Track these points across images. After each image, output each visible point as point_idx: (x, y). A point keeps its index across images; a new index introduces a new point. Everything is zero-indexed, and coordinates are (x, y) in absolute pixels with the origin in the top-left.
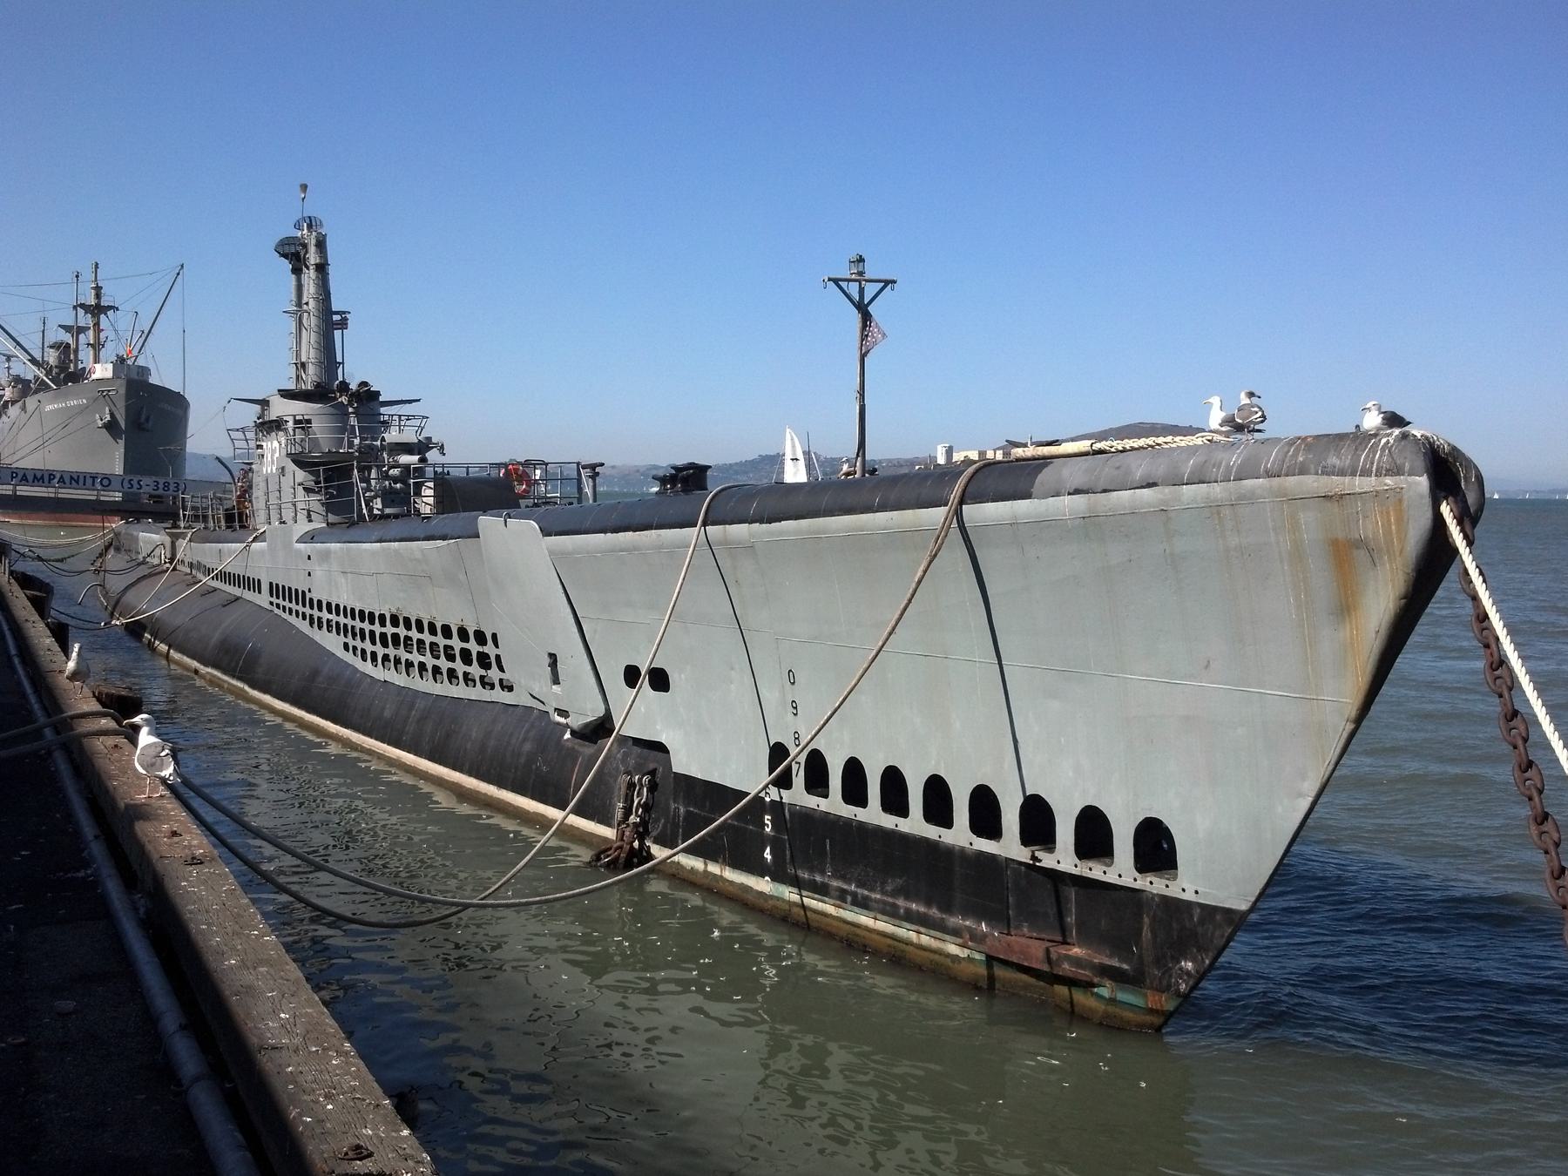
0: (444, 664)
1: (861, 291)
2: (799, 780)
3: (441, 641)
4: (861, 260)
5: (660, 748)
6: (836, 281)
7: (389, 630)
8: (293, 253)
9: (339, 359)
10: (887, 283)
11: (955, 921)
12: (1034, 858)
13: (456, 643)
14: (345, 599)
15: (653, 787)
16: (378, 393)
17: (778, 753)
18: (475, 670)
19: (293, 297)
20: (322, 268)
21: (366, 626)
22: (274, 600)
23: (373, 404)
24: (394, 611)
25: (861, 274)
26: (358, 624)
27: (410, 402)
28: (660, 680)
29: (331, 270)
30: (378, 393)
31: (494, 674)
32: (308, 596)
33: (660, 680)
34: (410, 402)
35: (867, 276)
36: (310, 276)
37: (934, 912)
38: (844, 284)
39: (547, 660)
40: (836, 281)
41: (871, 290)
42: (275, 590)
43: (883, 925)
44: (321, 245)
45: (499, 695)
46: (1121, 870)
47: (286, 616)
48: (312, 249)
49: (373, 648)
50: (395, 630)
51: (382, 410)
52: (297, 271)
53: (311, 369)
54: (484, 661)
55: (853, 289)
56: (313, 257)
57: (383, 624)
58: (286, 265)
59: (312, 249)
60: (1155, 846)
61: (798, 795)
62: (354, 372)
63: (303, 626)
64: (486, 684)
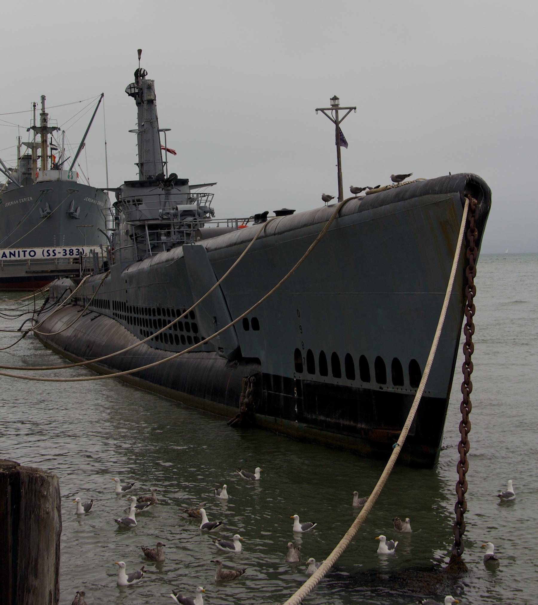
1: (337, 112)
2: (305, 367)
7: (157, 317)
9: (164, 160)
10: (351, 109)
12: (381, 388)
14: (141, 304)
17: (297, 353)
18: (192, 334)
22: (115, 311)
24: (158, 306)
27: (212, 184)
32: (127, 305)
33: (256, 325)
34: (212, 184)
40: (322, 110)
41: (342, 113)
44: (150, 87)
50: (159, 317)
51: (192, 191)
52: (138, 104)
57: (154, 315)
58: (132, 100)
61: (305, 376)
62: (174, 166)
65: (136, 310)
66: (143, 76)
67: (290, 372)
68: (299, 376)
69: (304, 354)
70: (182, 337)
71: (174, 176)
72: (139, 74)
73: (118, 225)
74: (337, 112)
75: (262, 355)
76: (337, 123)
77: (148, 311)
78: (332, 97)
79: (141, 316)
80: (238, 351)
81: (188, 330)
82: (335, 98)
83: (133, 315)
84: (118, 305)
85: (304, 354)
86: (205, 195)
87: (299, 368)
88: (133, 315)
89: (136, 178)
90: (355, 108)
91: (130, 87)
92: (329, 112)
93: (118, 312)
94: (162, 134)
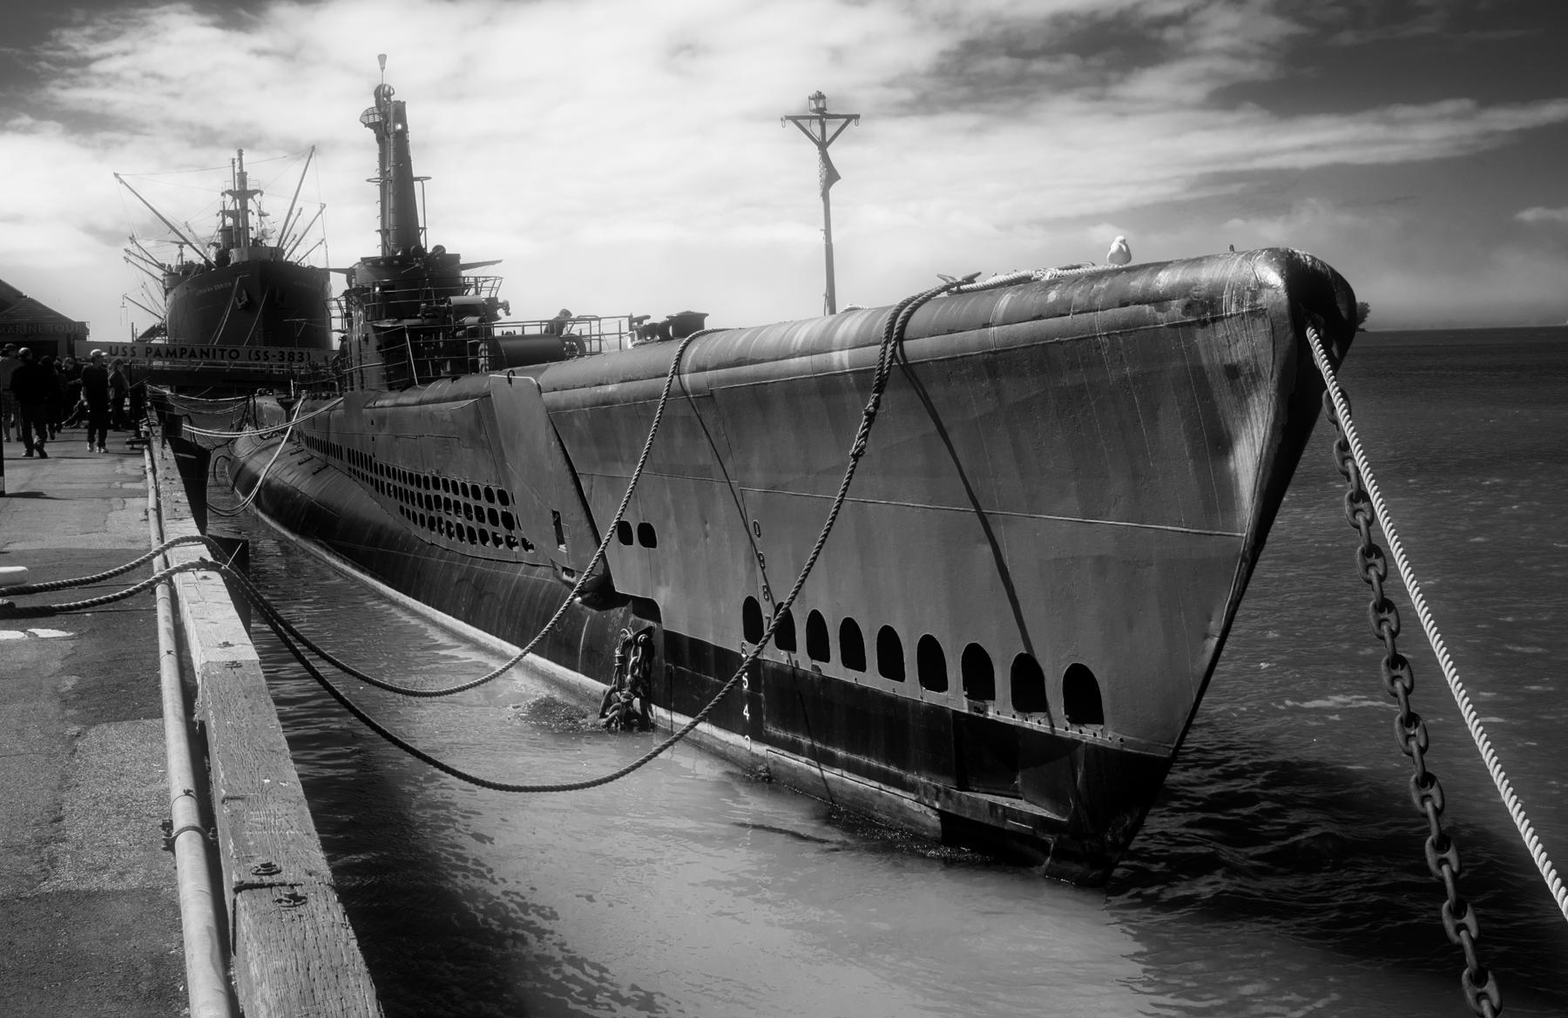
0: (474, 524)
3: (471, 501)
5: (647, 608)
7: (432, 492)
9: (421, 225)
11: (910, 777)
13: (484, 504)
15: (648, 647)
16: (457, 257)
18: (502, 531)
21: (414, 489)
28: (648, 537)
30: (457, 257)
33: (648, 537)
37: (893, 769)
38: (804, 122)
39: (551, 520)
43: (853, 781)
44: (400, 112)
51: (464, 273)
52: (380, 140)
54: (509, 521)
57: (427, 487)
58: (371, 134)
60: (1083, 695)
66: (388, 95)
67: (734, 640)
73: (350, 324)
75: (663, 597)
76: (823, 145)
77: (415, 479)
78: (813, 93)
84: (355, 457)
85: (767, 611)
86: (486, 279)
90: (857, 117)
91: (367, 114)
92: (804, 122)
93: (358, 469)
94: (417, 184)
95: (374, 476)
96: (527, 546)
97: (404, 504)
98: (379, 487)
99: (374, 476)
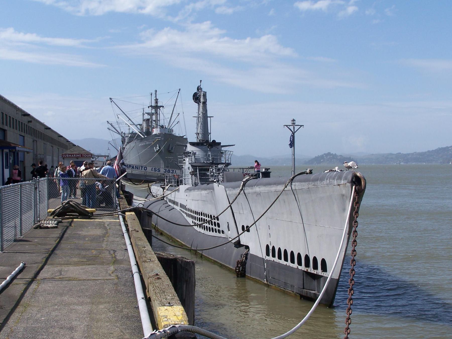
1: (294, 128)
4: (294, 120)
5: (247, 247)
6: (287, 126)
7: (201, 217)
8: (196, 98)
9: (209, 132)
10: (301, 126)
14: (193, 209)
17: (268, 247)
18: (217, 228)
19: (197, 111)
20: (205, 103)
21: (196, 215)
23: (219, 147)
25: (294, 124)
26: (196, 215)
29: (208, 103)
31: (221, 229)
35: (296, 124)
36: (201, 105)
40: (287, 126)
41: (296, 128)
42: (182, 206)
44: (205, 95)
45: (221, 235)
46: (319, 271)
47: (182, 213)
48: (202, 97)
49: (212, 226)
51: (223, 148)
53: (200, 135)
55: (292, 128)
56: (202, 100)
59: (202, 97)
61: (270, 258)
63: (185, 216)
64: (219, 231)
65: (191, 211)
68: (267, 258)
69: (271, 248)
70: (212, 228)
71: (214, 141)
72: (199, 89)
74: (294, 128)
79: (192, 214)
80: (239, 242)
81: (215, 226)
82: (294, 120)
83: (189, 213)
85: (271, 248)
87: (268, 254)
88: (189, 213)
89: (195, 141)
93: (182, 209)
95: (186, 211)
96: (223, 232)
97: (193, 220)
98: (188, 215)
99: (186, 211)
